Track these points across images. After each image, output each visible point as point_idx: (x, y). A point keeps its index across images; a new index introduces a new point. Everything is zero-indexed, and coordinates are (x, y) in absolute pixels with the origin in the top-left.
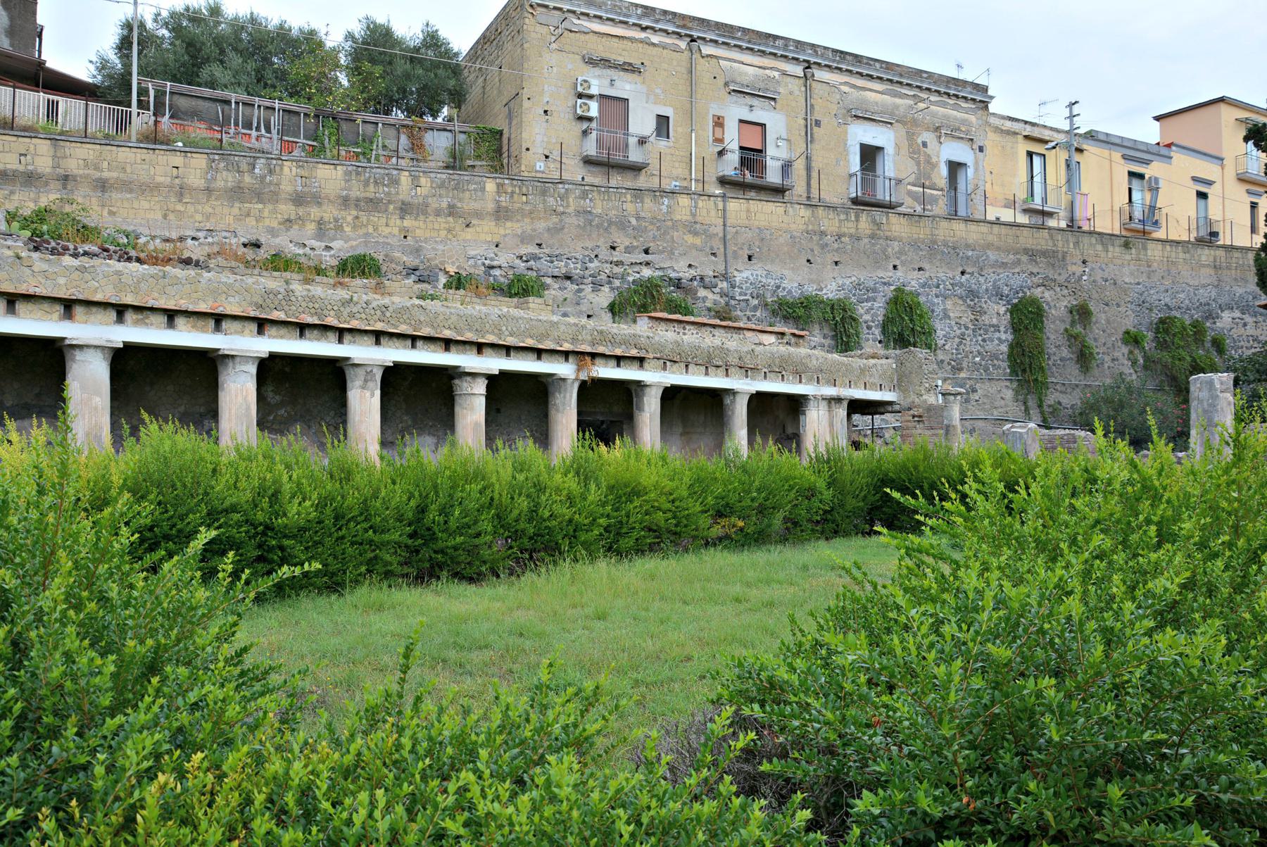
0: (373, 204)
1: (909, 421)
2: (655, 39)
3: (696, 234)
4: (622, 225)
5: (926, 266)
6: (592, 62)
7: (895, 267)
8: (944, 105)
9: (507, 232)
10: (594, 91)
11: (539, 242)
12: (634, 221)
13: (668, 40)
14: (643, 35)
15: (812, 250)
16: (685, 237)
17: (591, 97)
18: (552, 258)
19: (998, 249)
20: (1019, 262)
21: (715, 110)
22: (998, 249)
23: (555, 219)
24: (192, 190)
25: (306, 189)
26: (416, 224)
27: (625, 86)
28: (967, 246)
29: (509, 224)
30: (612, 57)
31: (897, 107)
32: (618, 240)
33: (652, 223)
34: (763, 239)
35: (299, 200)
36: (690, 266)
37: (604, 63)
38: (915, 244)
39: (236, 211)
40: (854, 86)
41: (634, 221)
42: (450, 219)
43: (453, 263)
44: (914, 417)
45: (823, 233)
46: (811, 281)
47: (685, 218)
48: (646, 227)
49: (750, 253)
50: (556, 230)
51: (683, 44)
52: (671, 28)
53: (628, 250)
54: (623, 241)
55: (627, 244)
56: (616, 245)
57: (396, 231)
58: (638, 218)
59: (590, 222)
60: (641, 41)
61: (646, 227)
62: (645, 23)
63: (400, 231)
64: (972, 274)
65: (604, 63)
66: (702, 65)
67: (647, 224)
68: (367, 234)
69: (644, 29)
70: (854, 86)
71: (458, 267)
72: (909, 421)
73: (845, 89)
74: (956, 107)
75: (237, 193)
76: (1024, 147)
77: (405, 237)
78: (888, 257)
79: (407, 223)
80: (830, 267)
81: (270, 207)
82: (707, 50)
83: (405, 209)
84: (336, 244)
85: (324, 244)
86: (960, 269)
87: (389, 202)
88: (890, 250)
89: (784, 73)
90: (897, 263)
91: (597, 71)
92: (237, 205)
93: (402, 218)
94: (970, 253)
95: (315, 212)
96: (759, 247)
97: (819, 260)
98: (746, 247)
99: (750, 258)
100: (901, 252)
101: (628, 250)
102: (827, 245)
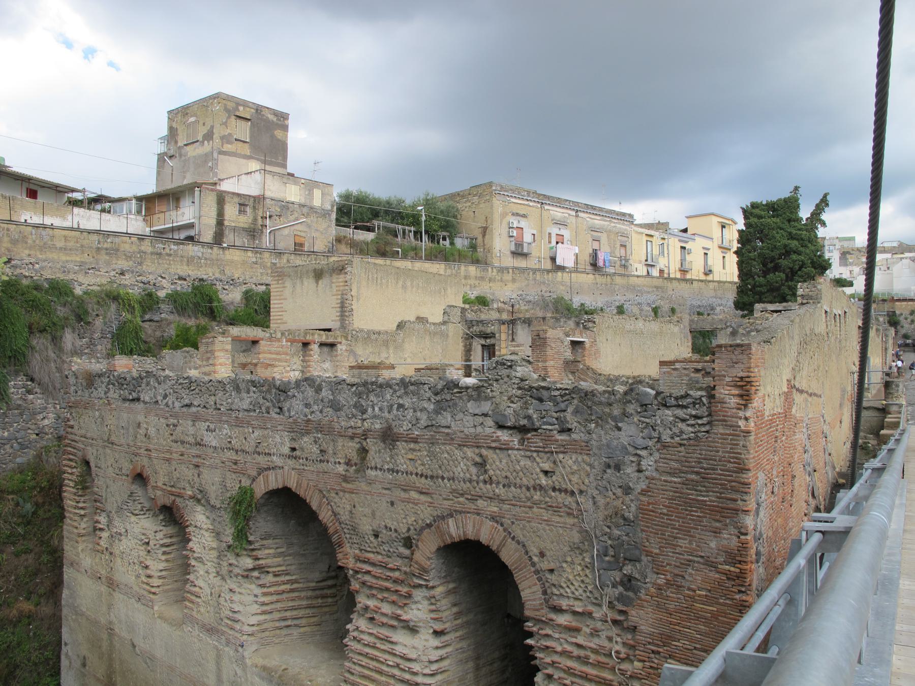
2: (531, 204)
6: (513, 214)
8: (619, 224)
10: (515, 226)
13: (535, 204)
14: (527, 203)
17: (512, 228)
21: (548, 230)
27: (523, 223)
30: (518, 212)
31: (604, 225)
37: (517, 214)
40: (591, 218)
51: (539, 206)
52: (536, 200)
60: (527, 205)
62: (529, 198)
65: (517, 214)
66: (544, 213)
69: (528, 200)
70: (591, 218)
73: (588, 219)
74: (623, 224)
76: (645, 238)
82: (546, 207)
89: (569, 215)
91: (514, 217)
95: (469, 282)
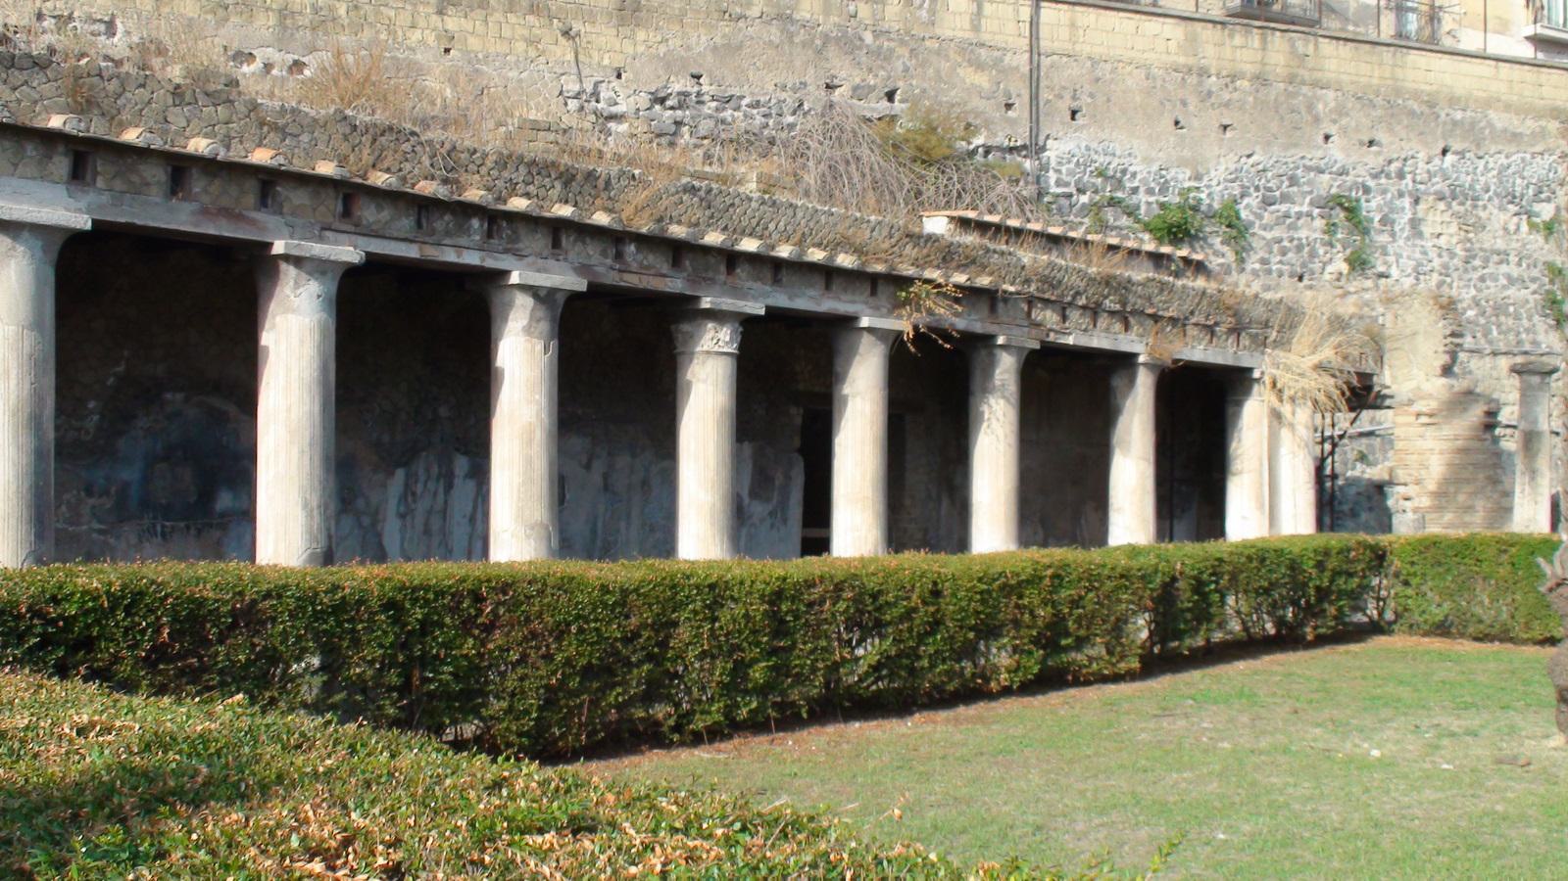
1: (1409, 425)
3: (980, 66)
5: (1381, 136)
7: (1327, 138)
9: (641, 49)
11: (695, 71)
12: (868, 37)
15: (1184, 103)
19: (1508, 107)
20: (1542, 134)
22: (1508, 107)
23: (725, 27)
26: (467, 25)
28: (1453, 101)
29: (641, 35)
32: (843, 74)
33: (902, 43)
34: (1098, 80)
38: (1363, 99)
41: (868, 37)
42: (531, 18)
44: (1418, 415)
45: (1203, 72)
46: (1182, 163)
47: (960, 34)
48: (891, 51)
49: (1075, 105)
50: (729, 50)
54: (848, 75)
55: (857, 80)
56: (836, 82)
57: (431, 39)
58: (877, 34)
59: (791, 36)
61: (891, 51)
63: (438, 38)
64: (1461, 154)
67: (892, 44)
72: (1409, 425)
77: (447, 51)
78: (1317, 120)
79: (453, 23)
80: (1214, 133)
86: (1441, 146)
88: (1320, 106)
90: (1332, 130)
94: (1459, 115)
96: (1091, 95)
97: (1196, 123)
98: (1067, 96)
99: (1074, 113)
100: (1341, 111)
101: (859, 92)
102: (1210, 94)
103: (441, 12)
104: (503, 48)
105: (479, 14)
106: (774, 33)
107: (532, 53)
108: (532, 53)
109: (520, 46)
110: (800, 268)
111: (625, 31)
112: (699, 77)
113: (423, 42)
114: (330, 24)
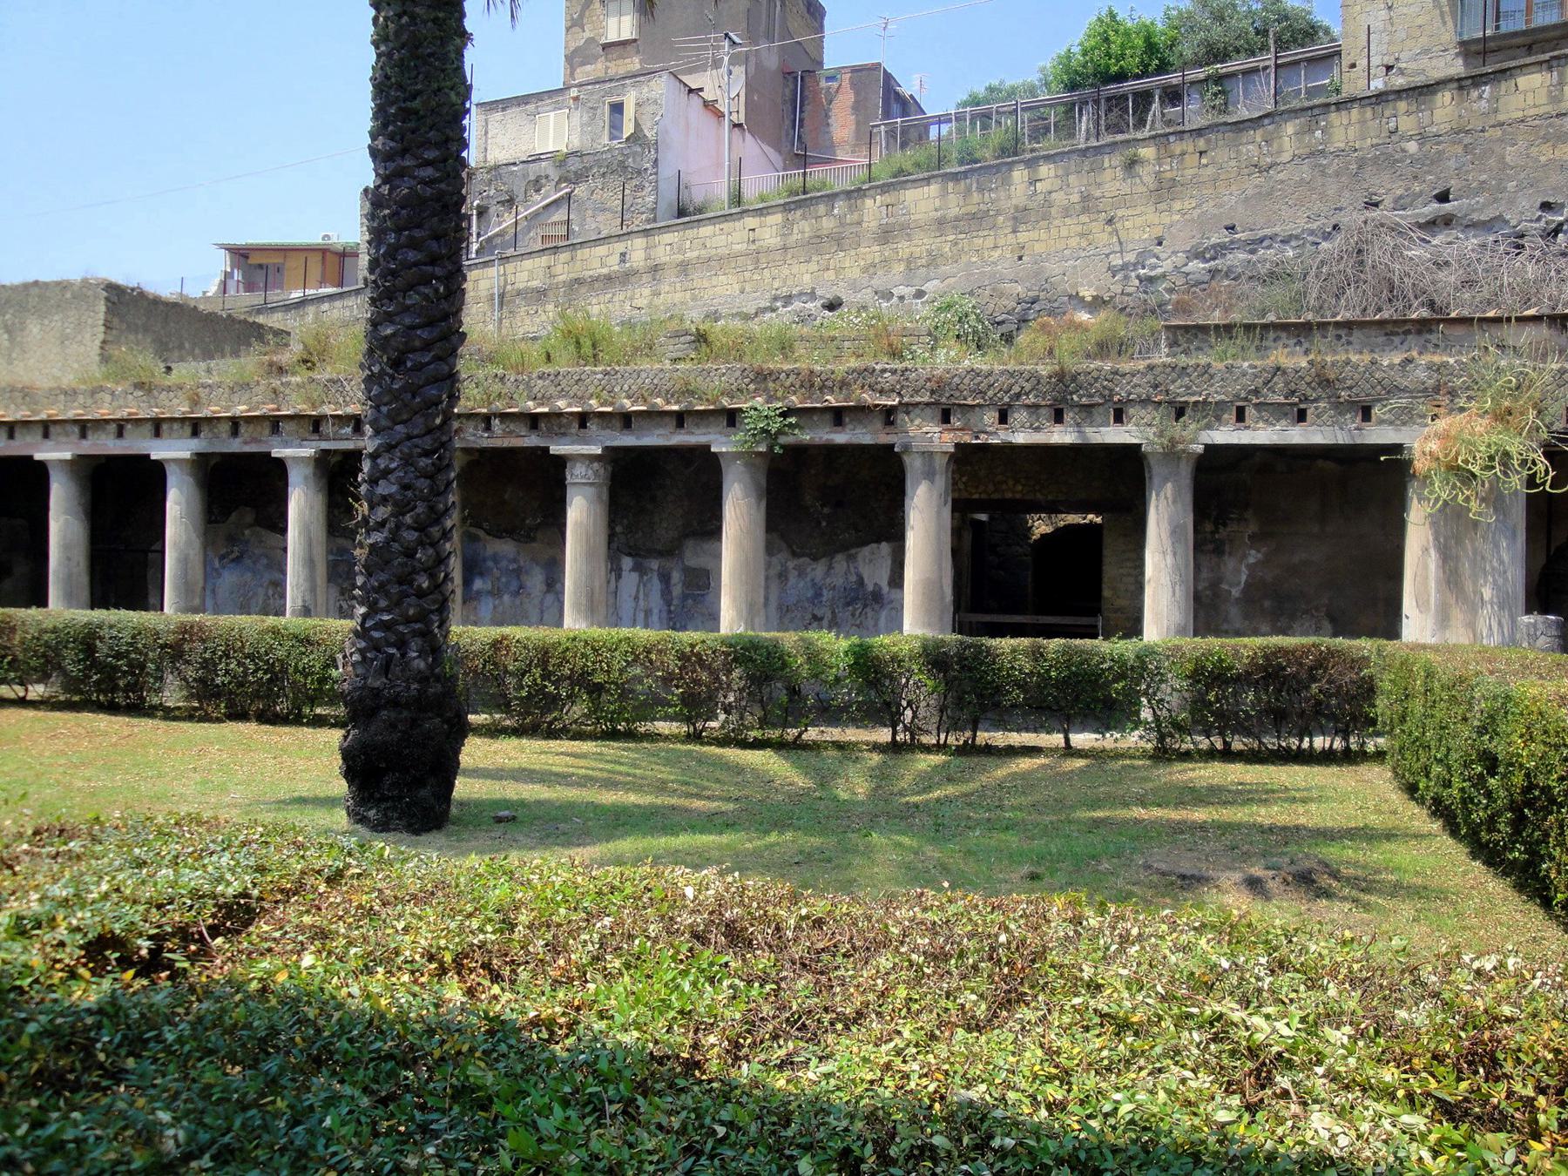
0: (976, 220)
4: (1387, 160)
9: (1176, 217)
11: (1228, 223)
16: (1534, 151)
18: (1254, 245)
24: (769, 251)
25: (892, 220)
26: (1034, 235)
29: (1177, 205)
35: (886, 235)
36: (1546, 206)
39: (813, 267)
42: (1084, 218)
43: (1090, 284)
53: (1399, 204)
54: (1388, 187)
55: (1399, 192)
68: (970, 264)
71: (1096, 290)
75: (816, 243)
77: (1020, 258)
79: (1023, 237)
81: (853, 252)
83: (1020, 217)
84: (928, 287)
85: (913, 290)
87: (998, 213)
92: (815, 258)
93: (1014, 231)
103: (1014, 231)
104: (1061, 245)
105: (1044, 223)
106: (1305, 171)
107: (1084, 244)
108: (1084, 244)
109: (1073, 242)
110: (654, 416)
111: (1162, 206)
112: (1233, 228)
113: (1001, 257)
114: (939, 261)
